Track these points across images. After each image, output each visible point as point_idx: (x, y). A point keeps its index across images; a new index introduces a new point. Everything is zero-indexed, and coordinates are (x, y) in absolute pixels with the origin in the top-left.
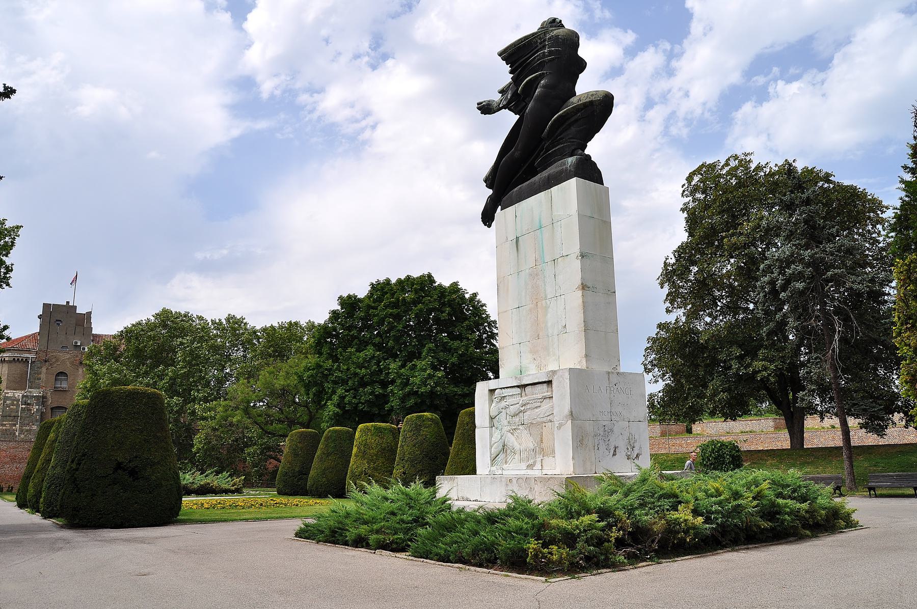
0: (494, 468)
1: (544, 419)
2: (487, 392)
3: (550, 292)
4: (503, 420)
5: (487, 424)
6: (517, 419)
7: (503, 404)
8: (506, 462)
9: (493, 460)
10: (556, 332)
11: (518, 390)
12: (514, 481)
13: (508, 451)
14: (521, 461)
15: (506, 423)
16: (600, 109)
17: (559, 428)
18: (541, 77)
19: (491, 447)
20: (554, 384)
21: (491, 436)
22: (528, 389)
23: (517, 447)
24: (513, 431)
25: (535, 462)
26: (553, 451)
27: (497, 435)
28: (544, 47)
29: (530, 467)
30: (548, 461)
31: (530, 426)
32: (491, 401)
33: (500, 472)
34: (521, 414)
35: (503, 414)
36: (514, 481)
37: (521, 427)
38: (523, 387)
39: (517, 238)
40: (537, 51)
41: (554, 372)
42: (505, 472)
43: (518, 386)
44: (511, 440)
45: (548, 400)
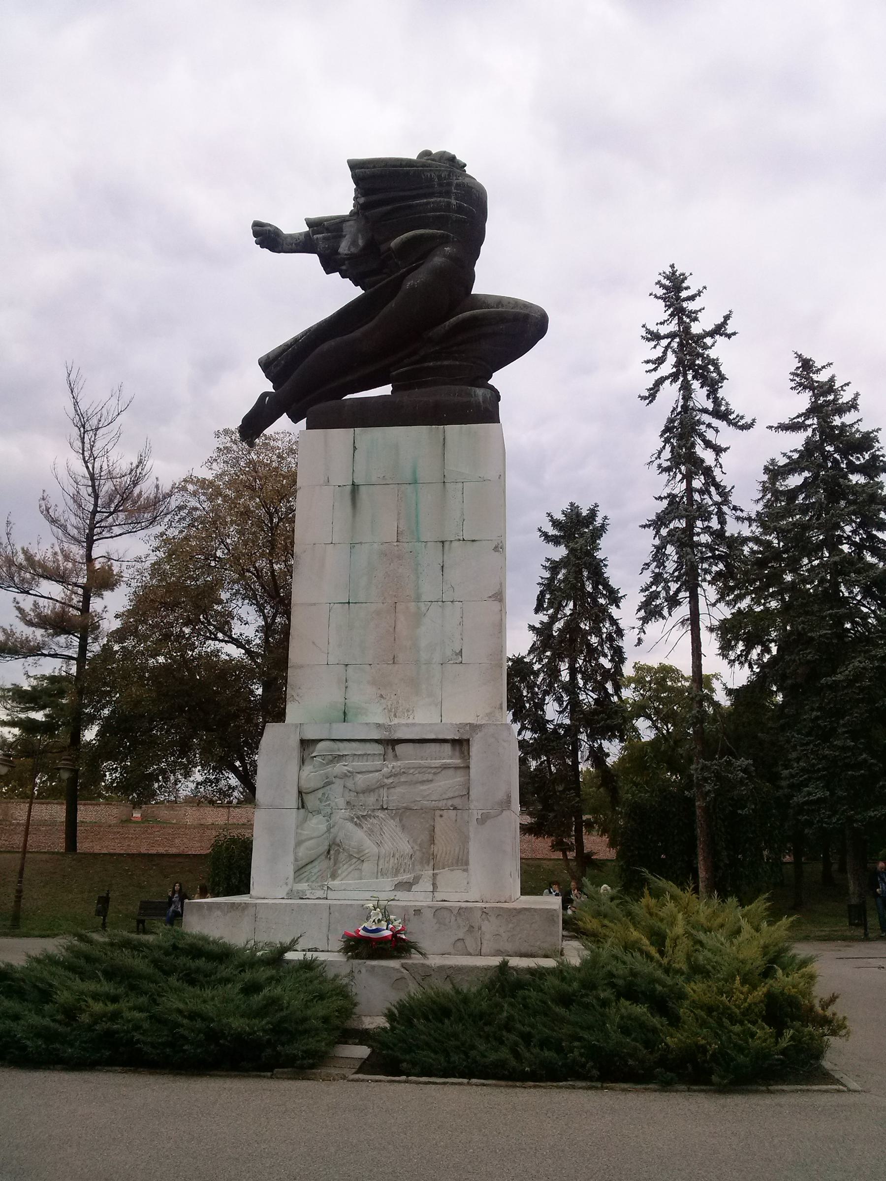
0: (303, 886)
1: (441, 804)
2: (294, 742)
3: (428, 591)
4: (338, 797)
5: (292, 799)
6: (371, 799)
7: (340, 768)
8: (334, 876)
9: (300, 871)
10: (437, 658)
11: (378, 749)
12: (428, 914)
13: (343, 856)
14: (383, 873)
15: (341, 802)
16: (520, 328)
17: (482, 821)
18: (445, 240)
19: (298, 844)
20: (475, 749)
21: (300, 824)
22: (399, 748)
23: (369, 846)
24: (359, 820)
25: (416, 880)
26: (462, 862)
27: (317, 825)
28: (448, 194)
29: (407, 886)
30: (446, 876)
31: (402, 813)
32: (303, 761)
33: (320, 893)
34: (383, 792)
35: (337, 787)
36: (428, 914)
37: (380, 814)
38: (393, 743)
39: (355, 488)
40: (432, 195)
41: (474, 728)
42: (331, 894)
43: (377, 741)
44: (357, 837)
45: (451, 772)
